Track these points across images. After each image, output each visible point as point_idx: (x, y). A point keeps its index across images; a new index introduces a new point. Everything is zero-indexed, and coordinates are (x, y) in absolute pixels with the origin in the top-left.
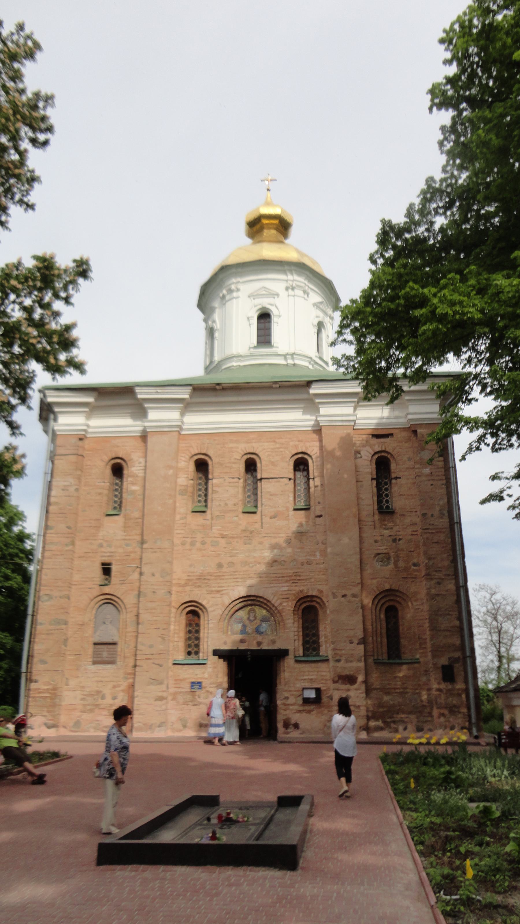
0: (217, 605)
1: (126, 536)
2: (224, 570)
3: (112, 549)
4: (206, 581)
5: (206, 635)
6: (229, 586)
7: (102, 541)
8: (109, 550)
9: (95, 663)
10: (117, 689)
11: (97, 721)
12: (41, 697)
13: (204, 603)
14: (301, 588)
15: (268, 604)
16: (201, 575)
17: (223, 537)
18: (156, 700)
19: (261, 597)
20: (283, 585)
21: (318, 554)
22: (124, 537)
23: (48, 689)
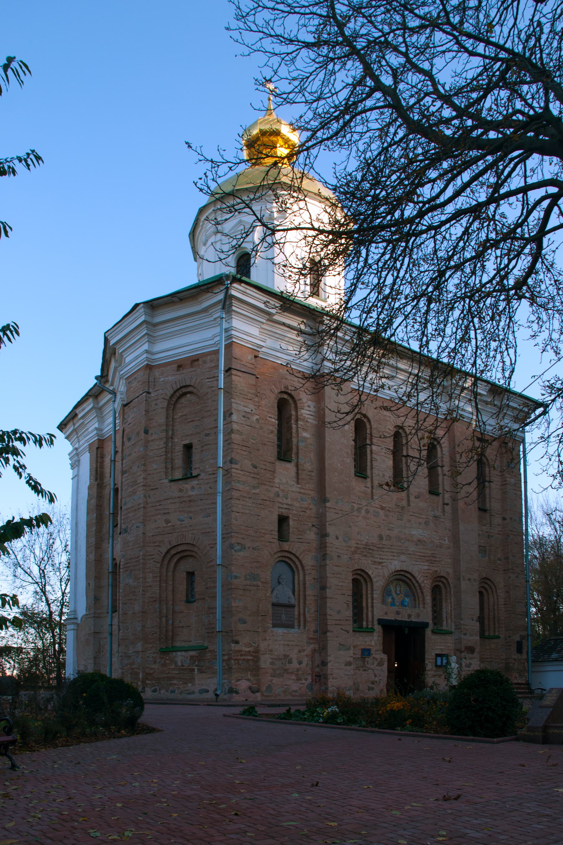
0: (379, 576)
1: (300, 488)
2: (384, 542)
3: (289, 501)
4: (371, 551)
5: (370, 605)
6: (387, 559)
7: (278, 489)
8: (285, 501)
9: (275, 626)
10: (302, 654)
11: (286, 685)
12: (244, 659)
13: (370, 573)
14: (436, 569)
15: (413, 580)
16: (367, 544)
17: (382, 508)
18: (346, 665)
19: (408, 572)
20: (426, 564)
21: (446, 539)
22: (298, 490)
23: (249, 652)
